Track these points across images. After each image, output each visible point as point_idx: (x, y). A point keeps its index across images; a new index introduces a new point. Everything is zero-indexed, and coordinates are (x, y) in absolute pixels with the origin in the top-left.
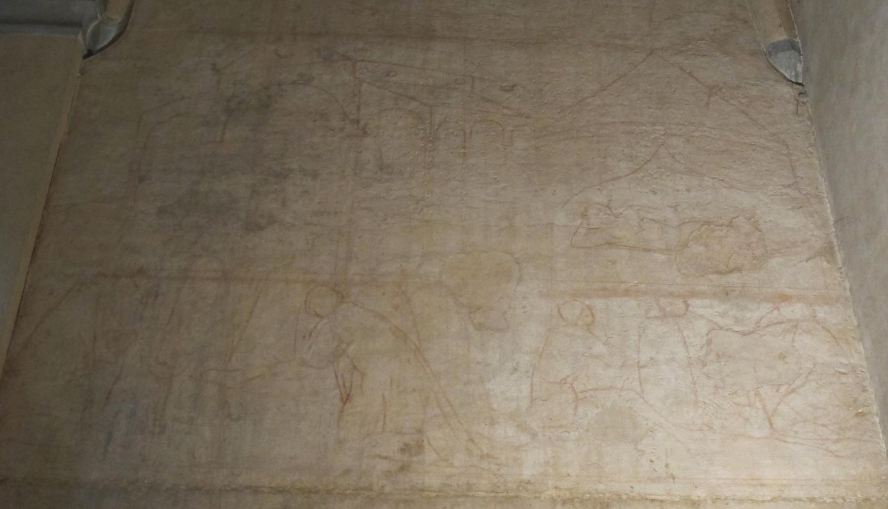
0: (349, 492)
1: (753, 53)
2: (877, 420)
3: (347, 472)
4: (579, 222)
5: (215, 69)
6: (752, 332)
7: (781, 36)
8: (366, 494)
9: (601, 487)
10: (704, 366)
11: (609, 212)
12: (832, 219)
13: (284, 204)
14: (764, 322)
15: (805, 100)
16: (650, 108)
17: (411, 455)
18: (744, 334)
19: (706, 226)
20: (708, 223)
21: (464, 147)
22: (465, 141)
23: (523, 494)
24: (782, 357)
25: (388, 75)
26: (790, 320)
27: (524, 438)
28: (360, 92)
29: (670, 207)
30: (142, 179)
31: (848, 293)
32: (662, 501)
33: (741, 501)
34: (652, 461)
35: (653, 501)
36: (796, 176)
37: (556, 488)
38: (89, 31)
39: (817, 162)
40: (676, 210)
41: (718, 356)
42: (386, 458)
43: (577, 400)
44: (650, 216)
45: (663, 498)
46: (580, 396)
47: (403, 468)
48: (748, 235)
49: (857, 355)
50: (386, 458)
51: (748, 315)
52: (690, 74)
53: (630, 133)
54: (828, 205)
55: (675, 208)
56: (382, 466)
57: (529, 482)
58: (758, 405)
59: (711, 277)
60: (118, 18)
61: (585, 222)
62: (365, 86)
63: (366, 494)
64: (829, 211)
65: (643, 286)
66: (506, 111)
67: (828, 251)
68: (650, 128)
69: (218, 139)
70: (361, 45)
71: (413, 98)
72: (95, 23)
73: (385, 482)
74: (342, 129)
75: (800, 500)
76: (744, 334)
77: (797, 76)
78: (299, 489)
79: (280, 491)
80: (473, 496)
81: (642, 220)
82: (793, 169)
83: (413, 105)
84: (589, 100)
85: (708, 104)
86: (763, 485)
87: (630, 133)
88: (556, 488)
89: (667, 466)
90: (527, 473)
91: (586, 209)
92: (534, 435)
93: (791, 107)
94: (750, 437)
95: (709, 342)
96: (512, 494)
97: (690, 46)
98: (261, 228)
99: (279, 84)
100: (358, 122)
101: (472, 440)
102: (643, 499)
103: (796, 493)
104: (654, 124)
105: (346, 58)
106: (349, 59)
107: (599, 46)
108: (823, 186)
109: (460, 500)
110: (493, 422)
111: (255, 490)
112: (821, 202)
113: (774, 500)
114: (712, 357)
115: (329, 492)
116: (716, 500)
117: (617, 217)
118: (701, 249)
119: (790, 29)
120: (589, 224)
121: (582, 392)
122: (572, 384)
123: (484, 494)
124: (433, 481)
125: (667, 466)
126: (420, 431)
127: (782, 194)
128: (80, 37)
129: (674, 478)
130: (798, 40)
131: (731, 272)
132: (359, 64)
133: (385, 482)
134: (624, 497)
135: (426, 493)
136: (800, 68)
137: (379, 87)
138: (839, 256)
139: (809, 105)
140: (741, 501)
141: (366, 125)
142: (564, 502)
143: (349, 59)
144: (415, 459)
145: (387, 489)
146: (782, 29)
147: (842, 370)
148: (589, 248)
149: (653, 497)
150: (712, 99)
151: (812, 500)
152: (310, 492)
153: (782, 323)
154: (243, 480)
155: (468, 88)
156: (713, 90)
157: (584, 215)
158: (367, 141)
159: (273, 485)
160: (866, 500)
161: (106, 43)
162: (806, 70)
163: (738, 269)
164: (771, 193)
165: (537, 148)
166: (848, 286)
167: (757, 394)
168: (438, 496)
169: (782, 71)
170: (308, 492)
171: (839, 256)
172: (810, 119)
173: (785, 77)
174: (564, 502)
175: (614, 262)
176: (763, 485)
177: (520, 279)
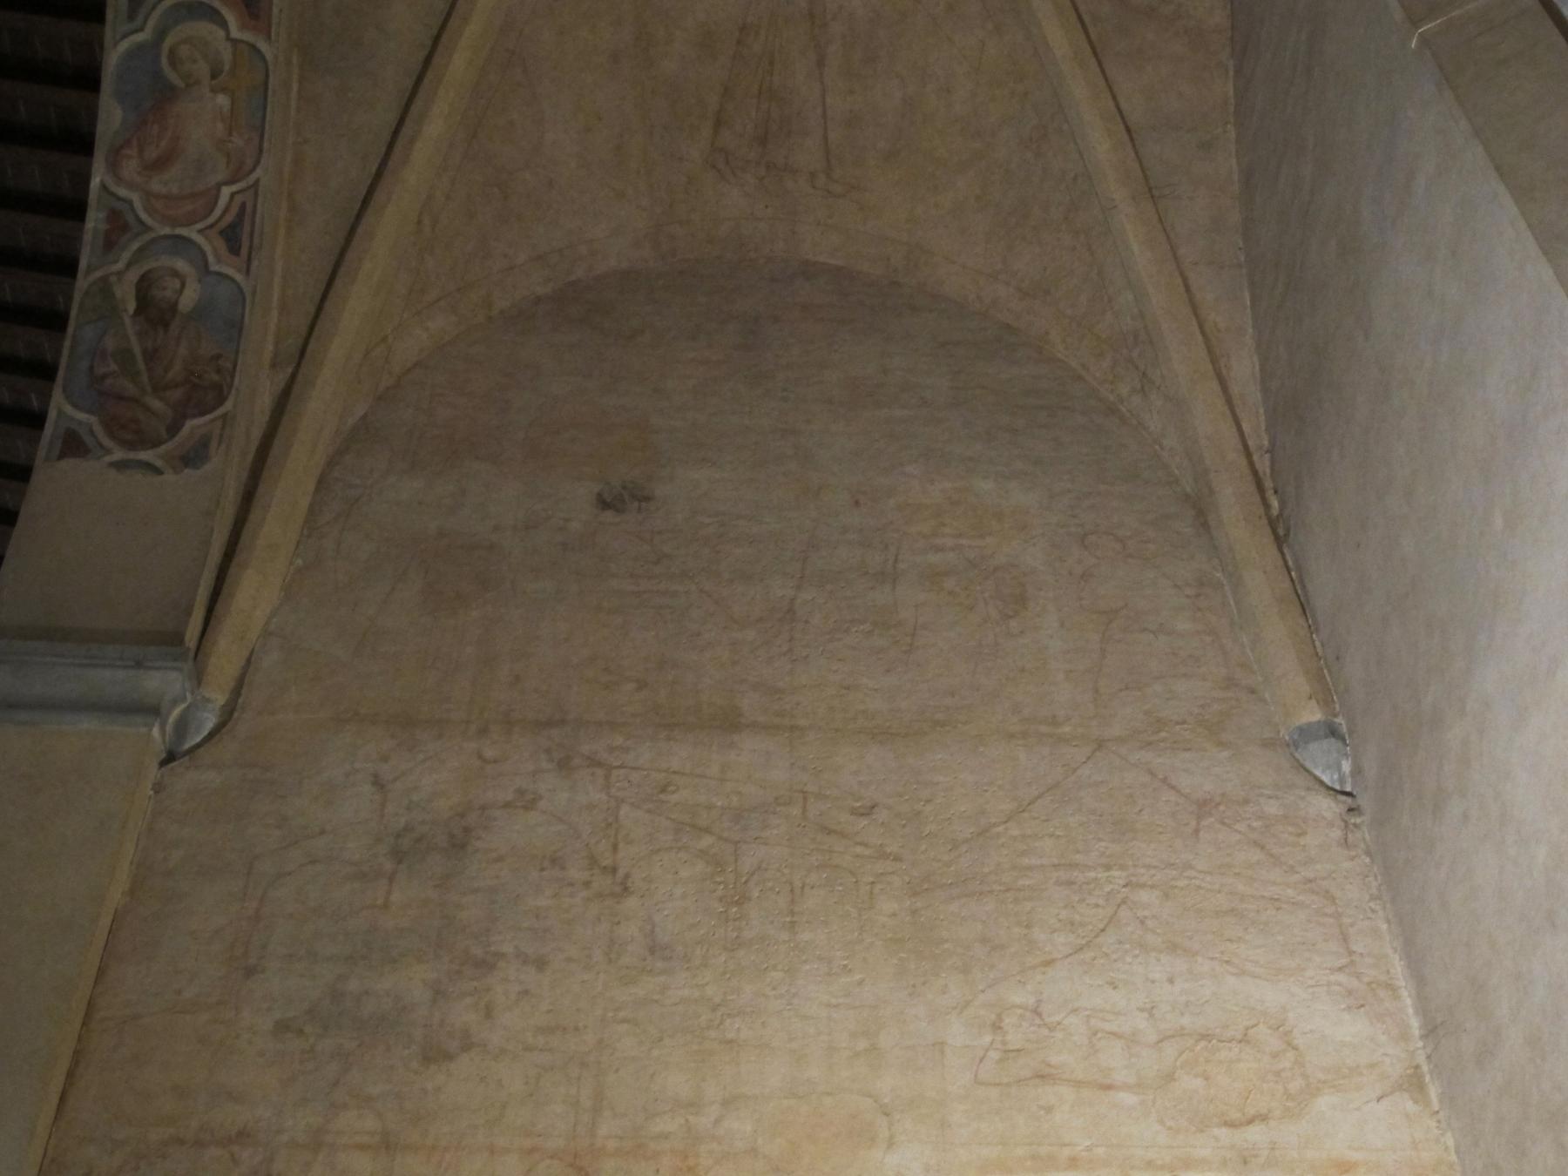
1: (1267, 744)
4: (988, 1039)
5: (378, 782)
7: (1312, 714)
11: (1038, 1021)
12: (1415, 1024)
13: (489, 1013)
15: (1358, 820)
16: (1100, 840)
19: (1203, 1044)
20: (1206, 1037)
21: (792, 913)
22: (793, 901)
25: (663, 790)
28: (617, 819)
29: (1142, 1010)
30: (250, 972)
31: (1454, 1157)
36: (1351, 953)
38: (171, 720)
39: (1385, 926)
40: (1151, 1015)
44: (1108, 1027)
48: (1275, 1056)
52: (1164, 780)
53: (1070, 883)
54: (1409, 1001)
55: (1150, 1011)
59: (1216, 1131)
60: (220, 699)
61: (999, 1038)
62: (625, 810)
64: (1411, 1011)
65: (1100, 1151)
66: (859, 849)
67: (1414, 1084)
68: (1102, 875)
69: (380, 902)
70: (619, 740)
71: (707, 830)
72: (183, 706)
74: (587, 884)
77: (1342, 780)
81: (1095, 1034)
82: (1345, 939)
83: (706, 841)
84: (1000, 829)
85: (1197, 831)
87: (1070, 883)
91: (1000, 1017)
93: (1336, 833)
97: (1163, 734)
98: (449, 1057)
99: (483, 808)
100: (614, 870)
104: (1108, 868)
105: (593, 762)
106: (599, 764)
107: (1012, 736)
108: (1398, 967)
112: (1397, 997)
117: (1052, 1029)
118: (1199, 1082)
119: (1326, 702)
120: (1004, 1043)
127: (1329, 984)
128: (156, 732)
130: (1339, 720)
131: (1250, 1122)
132: (615, 773)
136: (1346, 766)
137: (649, 811)
138: (1433, 1092)
139: (1365, 829)
141: (627, 876)
143: (599, 764)
146: (1313, 702)
148: (1008, 1085)
150: (1204, 823)
155: (796, 811)
156: (1204, 807)
157: (997, 1027)
158: (632, 903)
161: (198, 739)
162: (1357, 771)
163: (1263, 1118)
164: (1310, 982)
165: (914, 912)
166: (1451, 1142)
169: (1318, 773)
171: (1433, 1092)
172: (1368, 853)
173: (1322, 783)
175: (1049, 1110)
177: (891, 1144)
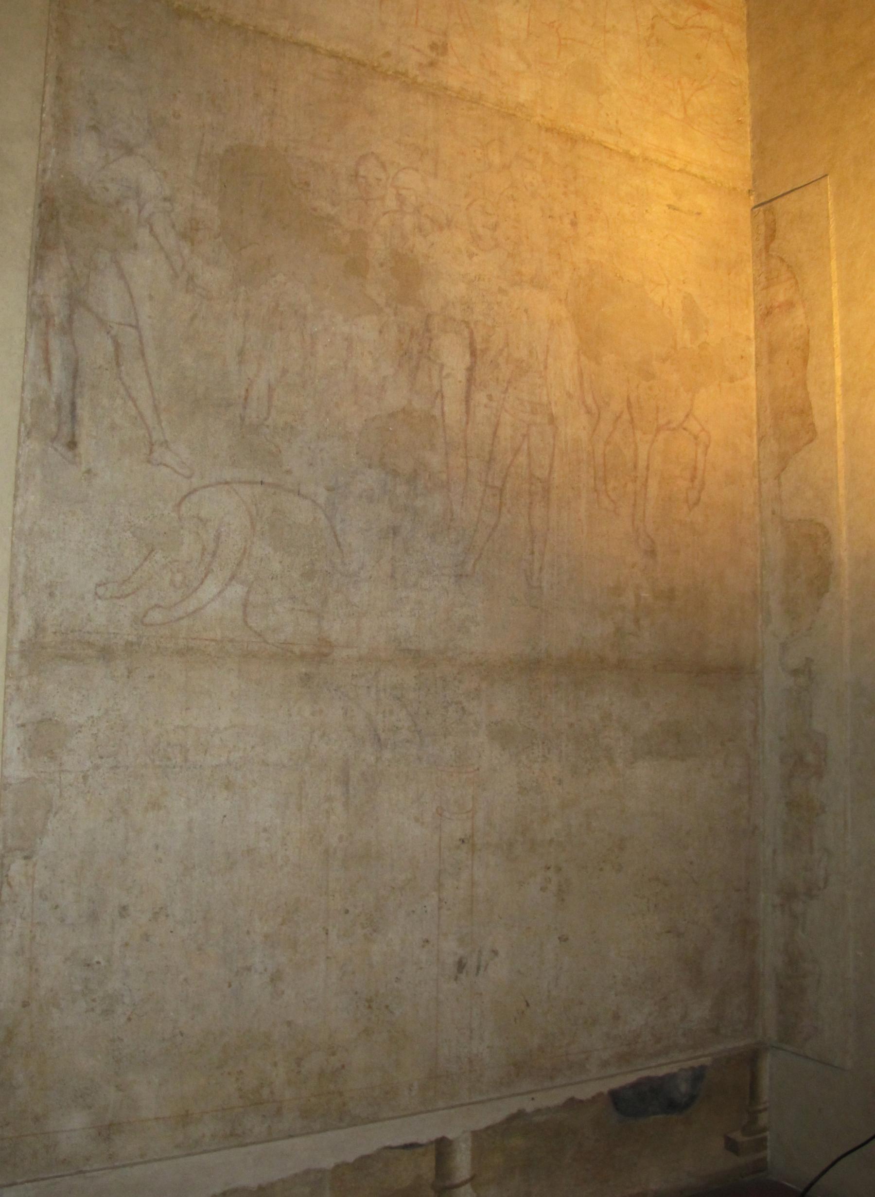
0: (390, 73)
2: (749, 129)
3: (388, 54)
6: (681, 29)
8: (403, 79)
9: (573, 125)
10: (648, 46)
14: (690, 23)
17: (438, 54)
18: (677, 28)
23: (519, 114)
24: (698, 57)
26: (706, 27)
27: (522, 66)
32: (611, 150)
33: (661, 165)
34: (608, 115)
35: (605, 147)
37: (542, 116)
41: (658, 41)
42: (418, 50)
43: (560, 44)
45: (613, 147)
46: (563, 42)
47: (432, 64)
49: (742, 73)
50: (418, 50)
51: (681, 12)
56: (416, 57)
57: (523, 105)
58: (679, 91)
63: (403, 79)
73: (418, 73)
75: (696, 176)
76: (677, 28)
78: (350, 59)
79: (333, 55)
80: (483, 105)
86: (675, 157)
88: (542, 116)
89: (617, 122)
90: (523, 98)
92: (529, 66)
94: (671, 116)
95: (653, 27)
96: (511, 112)
101: (483, 55)
102: (600, 143)
103: (694, 170)
109: (474, 105)
110: (500, 45)
111: (314, 49)
113: (680, 171)
114: (653, 40)
115: (374, 68)
116: (646, 159)
121: (565, 39)
122: (557, 29)
123: (491, 106)
124: (454, 83)
125: (617, 122)
126: (445, 34)
129: (621, 133)
133: (418, 73)
134: (587, 138)
135: (449, 92)
140: (661, 165)
142: (547, 130)
144: (441, 59)
145: (420, 80)
147: (734, 82)
149: (606, 144)
151: (703, 178)
152: (359, 63)
153: (701, 28)
154: (302, 36)
159: (328, 48)
160: (735, 189)
167: (679, 82)
168: (457, 97)
170: (360, 64)
174: (547, 130)
176: (675, 157)
